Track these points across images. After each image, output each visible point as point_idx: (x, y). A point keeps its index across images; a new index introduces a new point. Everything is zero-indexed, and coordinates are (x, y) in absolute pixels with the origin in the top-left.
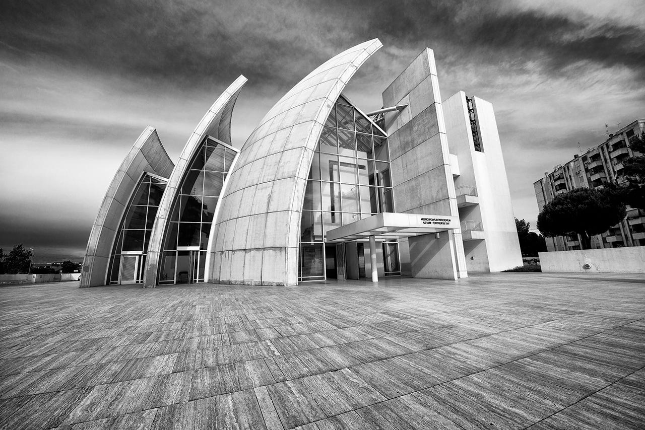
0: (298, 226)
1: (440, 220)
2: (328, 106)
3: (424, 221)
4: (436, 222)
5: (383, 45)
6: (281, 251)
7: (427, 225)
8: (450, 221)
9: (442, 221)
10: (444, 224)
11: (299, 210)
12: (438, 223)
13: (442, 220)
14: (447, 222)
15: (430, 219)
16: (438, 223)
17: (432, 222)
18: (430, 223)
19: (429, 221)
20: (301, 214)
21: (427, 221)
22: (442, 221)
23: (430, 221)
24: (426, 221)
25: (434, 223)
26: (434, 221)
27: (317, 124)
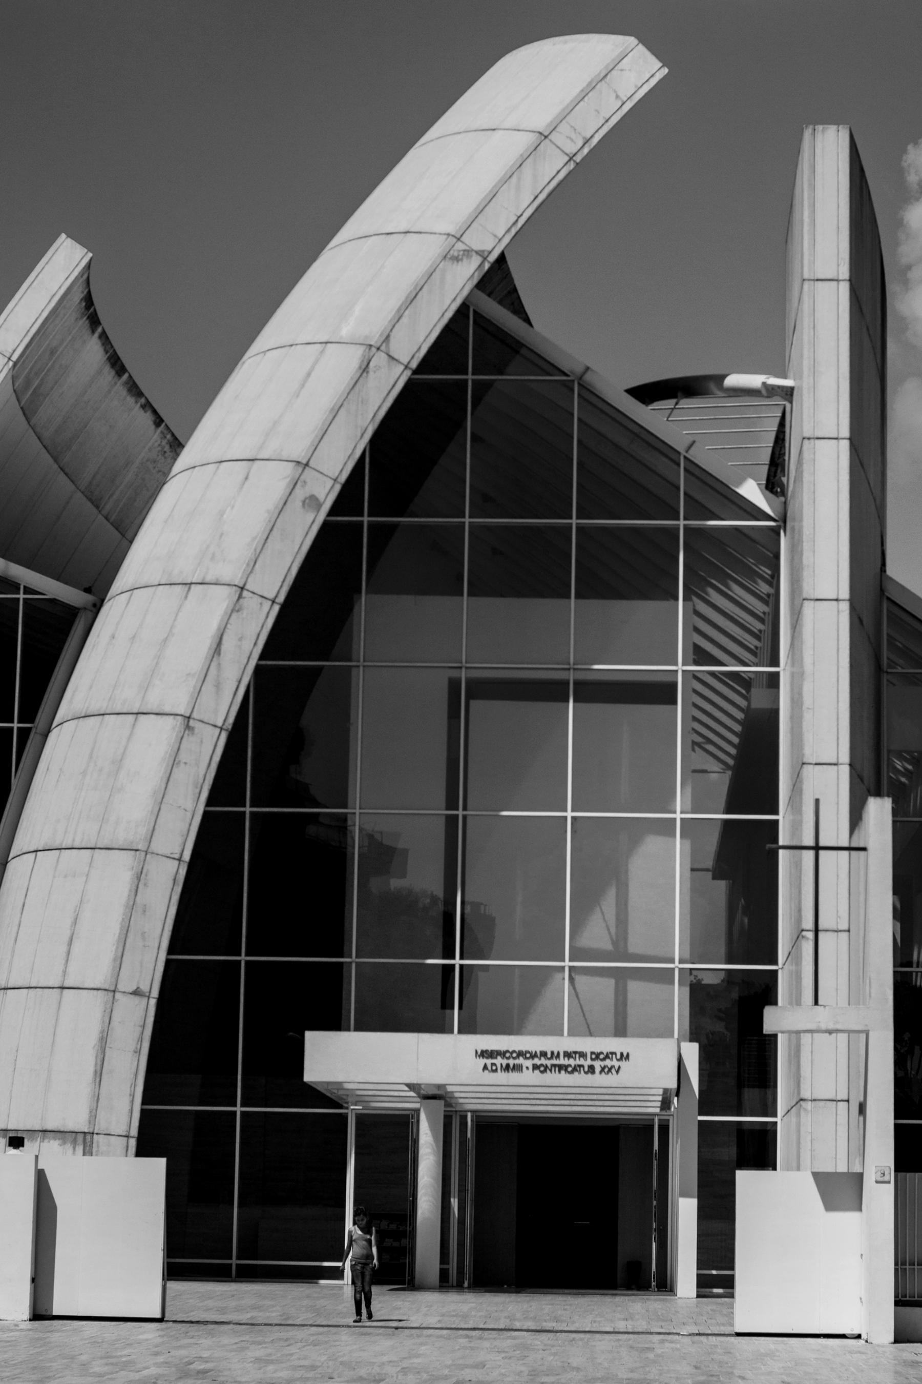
0: (138, 1052)
1: (568, 1055)
2: (312, 502)
3: (489, 1062)
4: (549, 1063)
5: (666, 71)
6: (74, 1148)
7: (502, 1077)
8: (624, 1057)
9: (581, 1062)
10: (592, 1069)
11: (145, 987)
12: (561, 1068)
13: (582, 1055)
14: (608, 1063)
15: (520, 1054)
16: (561, 1068)
17: (529, 1063)
18: (518, 1068)
19: (511, 1062)
20: (153, 1002)
21: (505, 1062)
22: (581, 1062)
23: (521, 1061)
24: (499, 1061)
25: (535, 1067)
26: (543, 1061)
27: (249, 601)
